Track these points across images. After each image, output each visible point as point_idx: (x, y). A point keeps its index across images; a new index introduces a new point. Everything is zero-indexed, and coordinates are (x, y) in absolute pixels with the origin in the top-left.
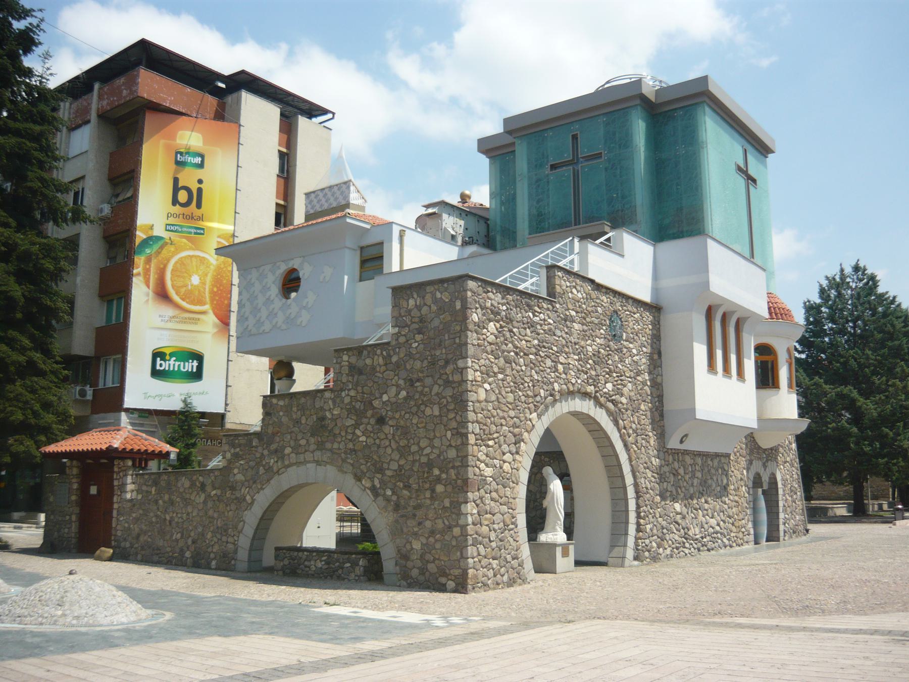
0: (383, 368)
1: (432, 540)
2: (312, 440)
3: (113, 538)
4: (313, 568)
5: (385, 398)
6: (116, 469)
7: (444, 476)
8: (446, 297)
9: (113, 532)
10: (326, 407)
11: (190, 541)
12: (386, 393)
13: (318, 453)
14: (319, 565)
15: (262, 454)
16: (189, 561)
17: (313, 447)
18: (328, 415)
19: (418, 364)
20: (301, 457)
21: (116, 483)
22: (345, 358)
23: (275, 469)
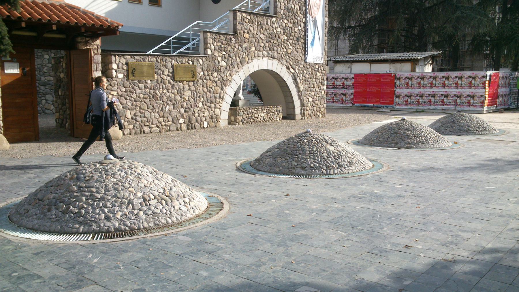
2: (267, 44)
11: (182, 110)
14: (263, 115)
16: (184, 127)
18: (275, 31)
20: (260, 53)
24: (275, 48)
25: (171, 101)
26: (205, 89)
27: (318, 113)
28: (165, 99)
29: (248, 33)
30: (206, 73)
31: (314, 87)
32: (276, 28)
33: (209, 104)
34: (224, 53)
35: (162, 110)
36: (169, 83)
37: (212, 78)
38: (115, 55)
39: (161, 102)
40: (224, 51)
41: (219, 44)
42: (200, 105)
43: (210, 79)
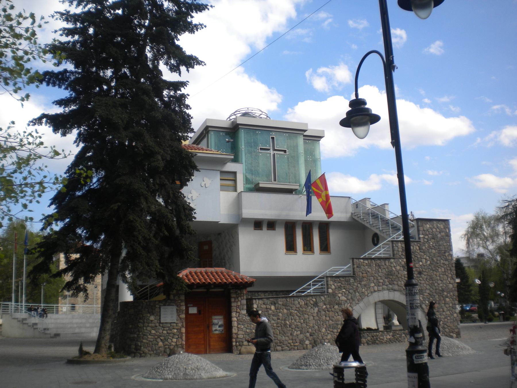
0: (419, 251)
1: (446, 320)
2: (386, 280)
3: (234, 340)
4: (385, 339)
5: (421, 263)
6: (233, 295)
7: (449, 295)
8: (442, 226)
9: (234, 336)
10: (392, 265)
11: (308, 334)
12: (422, 261)
13: (391, 286)
14: (389, 337)
15: (357, 286)
17: (388, 283)
18: (393, 268)
19: (434, 251)
20: (380, 288)
21: (233, 304)
22: (400, 244)
23: (366, 294)
24: (395, 282)
25: (298, 328)
26: (328, 319)
27: (452, 334)
28: (293, 326)
29: (366, 273)
30: (328, 306)
31: (444, 311)
32: (394, 267)
33: (331, 330)
34: (344, 290)
35: (291, 334)
36: (297, 315)
37: (333, 309)
38: (255, 299)
39: (290, 329)
40: (344, 289)
41: (339, 284)
42: (324, 330)
43: (332, 311)
